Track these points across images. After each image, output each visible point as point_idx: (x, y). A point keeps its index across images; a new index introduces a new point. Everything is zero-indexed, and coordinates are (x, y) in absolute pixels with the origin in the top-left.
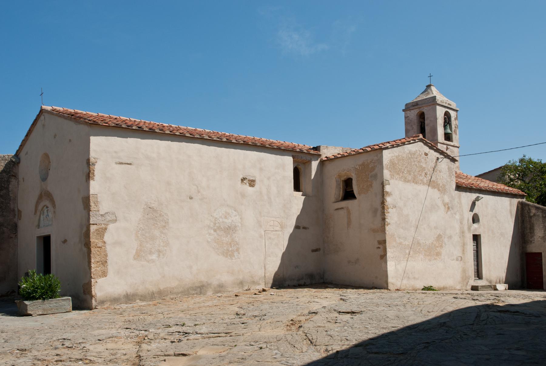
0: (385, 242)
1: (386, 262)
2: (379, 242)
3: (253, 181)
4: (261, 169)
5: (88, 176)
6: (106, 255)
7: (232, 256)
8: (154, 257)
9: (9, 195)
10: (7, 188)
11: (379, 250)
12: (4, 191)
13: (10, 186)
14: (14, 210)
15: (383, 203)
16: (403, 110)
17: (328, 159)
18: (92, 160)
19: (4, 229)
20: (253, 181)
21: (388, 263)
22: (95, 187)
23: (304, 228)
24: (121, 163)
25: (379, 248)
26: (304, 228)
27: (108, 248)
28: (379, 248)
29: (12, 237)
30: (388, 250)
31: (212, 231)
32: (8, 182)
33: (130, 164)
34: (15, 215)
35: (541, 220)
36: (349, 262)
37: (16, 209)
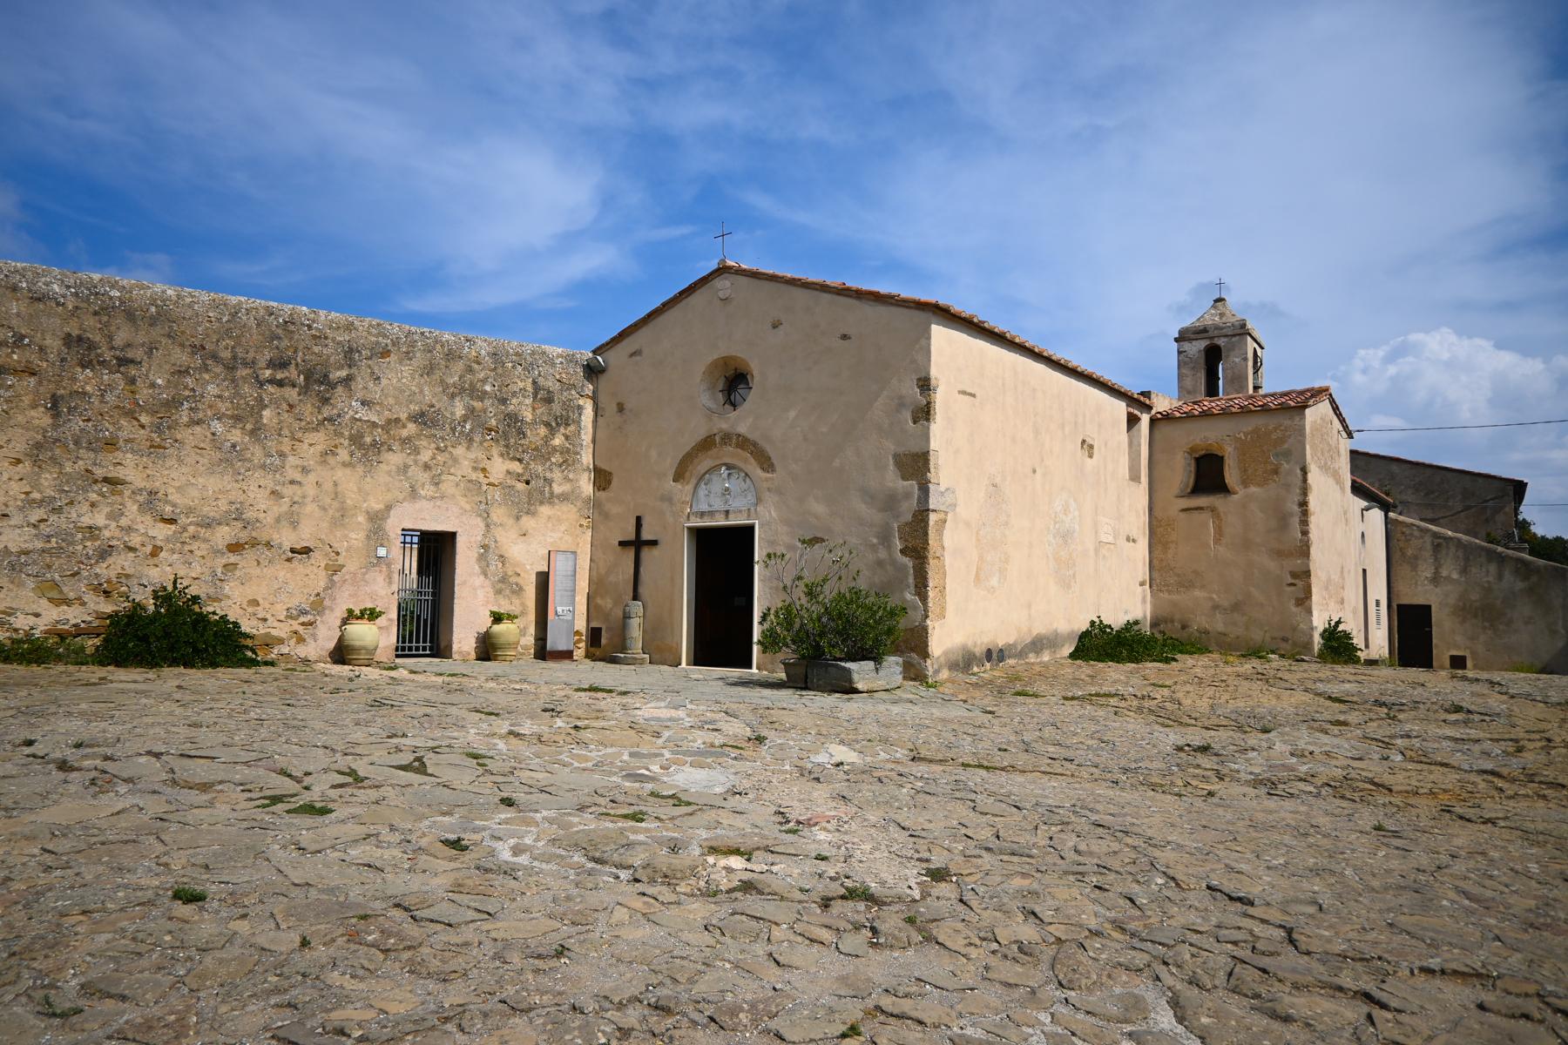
0: (1308, 573)
1: (1310, 612)
2: (1294, 575)
3: (1091, 447)
4: (1100, 426)
5: (924, 413)
6: (945, 574)
7: (1069, 587)
8: (994, 582)
15: (1304, 504)
16: (1176, 340)
17: (1167, 417)
18: (933, 382)
21: (1315, 613)
22: (941, 437)
27: (948, 560)
30: (1314, 590)
33: (974, 396)
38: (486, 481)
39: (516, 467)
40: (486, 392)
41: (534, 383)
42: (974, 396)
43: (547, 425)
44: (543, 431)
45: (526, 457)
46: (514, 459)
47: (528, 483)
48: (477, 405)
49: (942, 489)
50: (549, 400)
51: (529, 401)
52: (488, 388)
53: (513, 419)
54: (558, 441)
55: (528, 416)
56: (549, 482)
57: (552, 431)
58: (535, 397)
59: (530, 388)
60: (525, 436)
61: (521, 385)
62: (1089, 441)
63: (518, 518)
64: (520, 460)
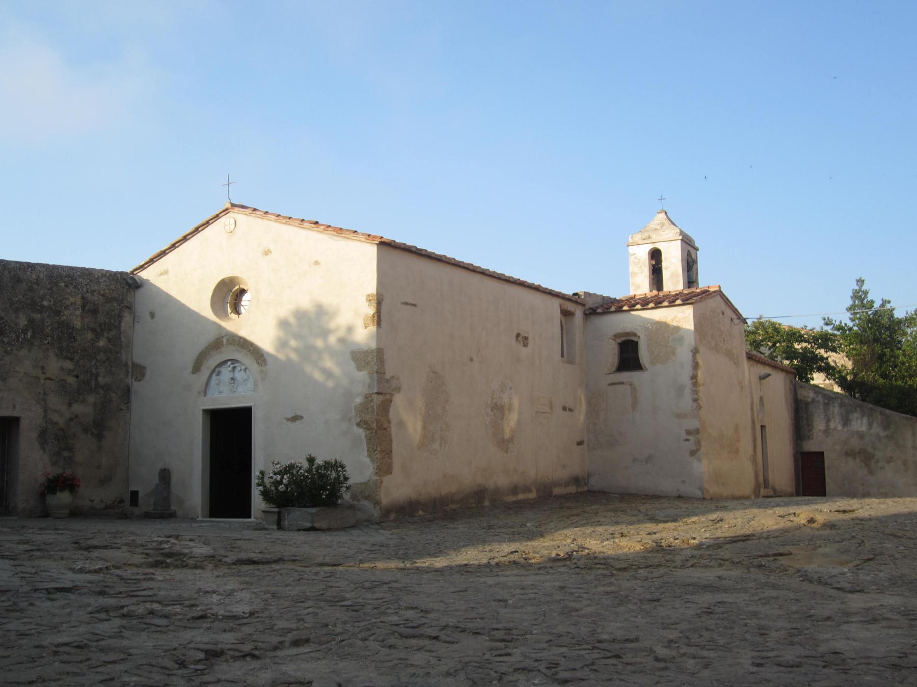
3: (526, 338)
9: (120, 339)
10: (118, 327)
11: (687, 443)
12: (114, 332)
13: (123, 324)
14: (126, 365)
19: (113, 395)
20: (526, 338)
23: (570, 410)
24: (406, 304)
25: (687, 440)
26: (570, 410)
28: (687, 440)
29: (122, 410)
30: (703, 443)
31: (489, 410)
32: (120, 316)
33: (415, 305)
34: (128, 372)
35: (821, 407)
36: (635, 460)
37: (130, 363)
38: (45, 376)
39: (68, 365)
40: (43, 306)
41: (83, 298)
42: (415, 305)
43: (93, 330)
44: (90, 335)
45: (77, 357)
46: (67, 358)
47: (77, 377)
48: (37, 316)
49: (388, 376)
50: (95, 312)
51: (78, 312)
52: (45, 303)
53: (66, 326)
54: (101, 343)
55: (78, 324)
56: (97, 375)
57: (98, 335)
58: (83, 307)
59: (79, 301)
60: (75, 340)
61: (72, 300)
62: (524, 334)
63: (70, 405)
64: (71, 359)
